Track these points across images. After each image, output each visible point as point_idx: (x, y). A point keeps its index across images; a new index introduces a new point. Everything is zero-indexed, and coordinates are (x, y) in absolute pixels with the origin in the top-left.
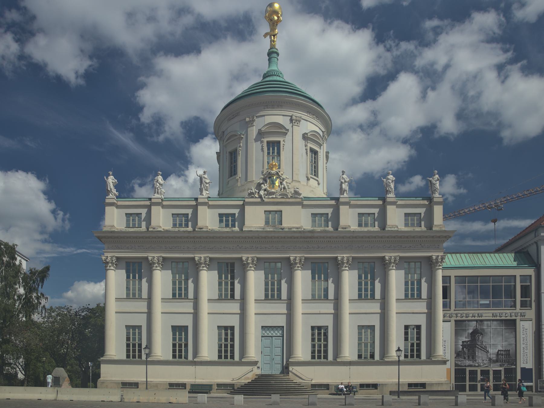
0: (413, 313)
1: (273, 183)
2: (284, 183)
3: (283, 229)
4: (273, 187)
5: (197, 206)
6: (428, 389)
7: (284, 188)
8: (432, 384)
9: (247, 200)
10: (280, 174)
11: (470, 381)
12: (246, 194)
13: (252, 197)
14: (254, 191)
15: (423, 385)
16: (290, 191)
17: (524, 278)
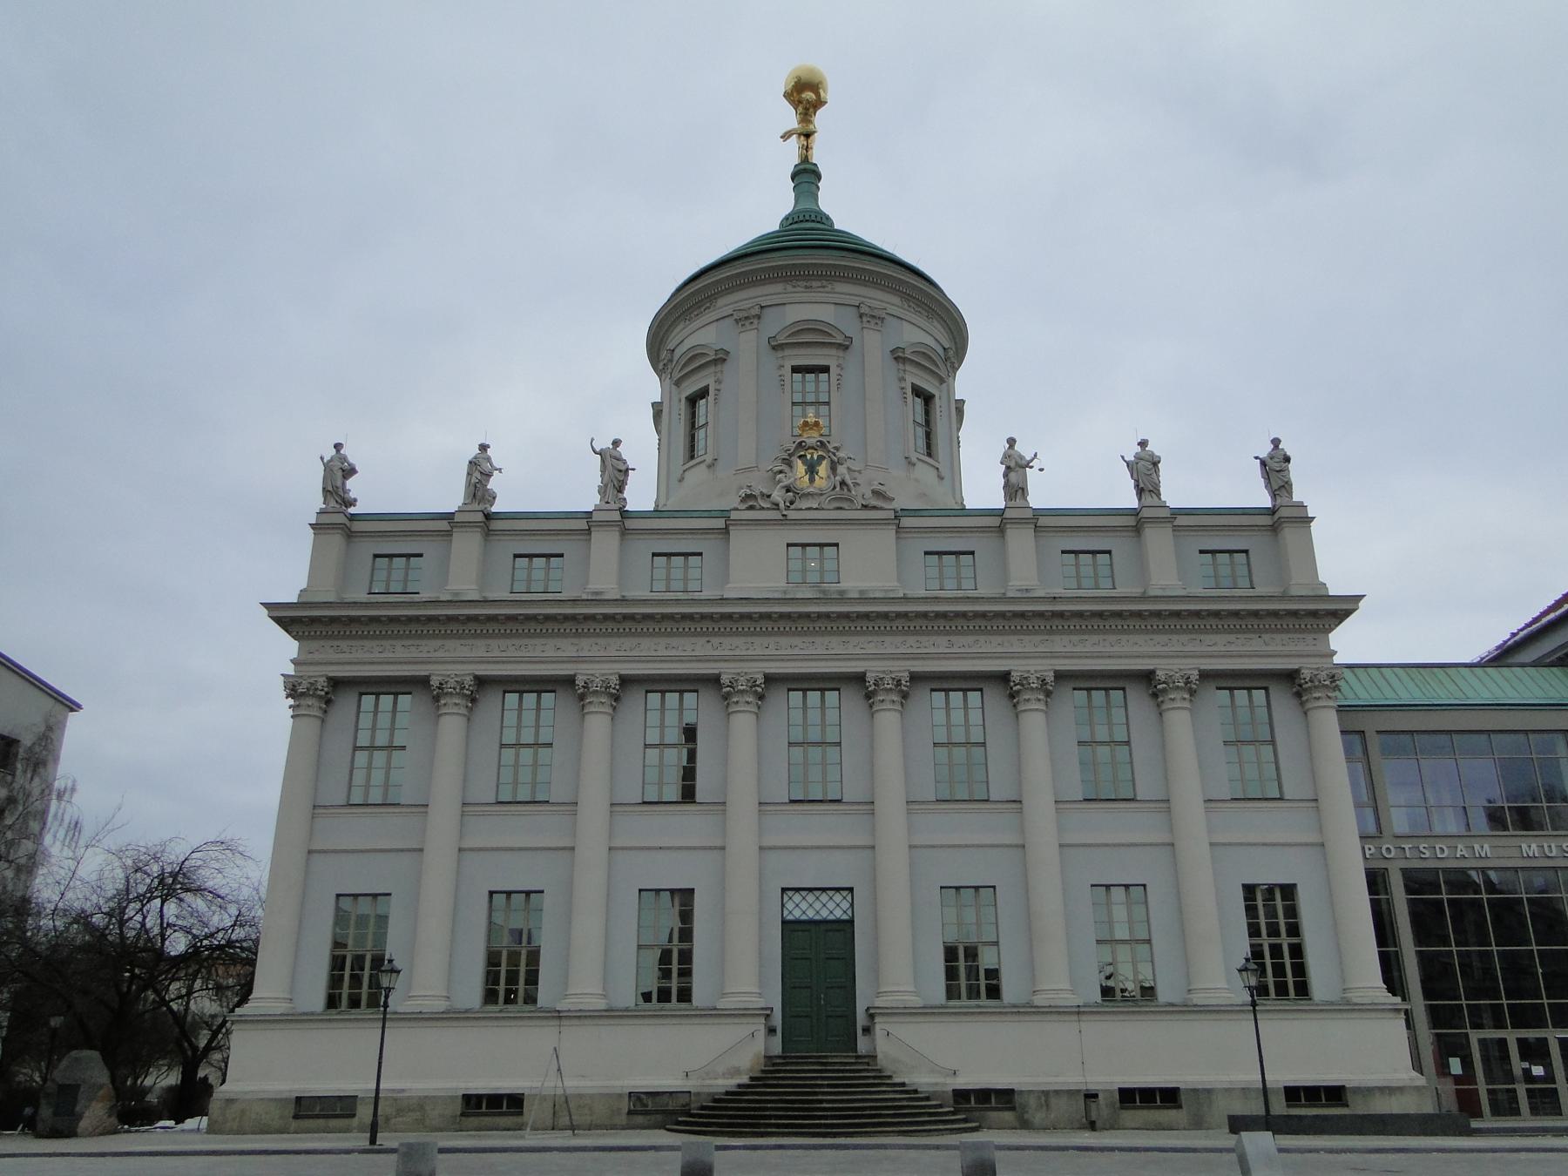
0: (1264, 844)
1: (812, 470)
2: (841, 469)
3: (842, 592)
4: (812, 480)
6: (1358, 1107)
7: (843, 483)
8: (1367, 1092)
9: (734, 515)
10: (830, 447)
12: (735, 502)
13: (751, 508)
14: (756, 493)
15: (1335, 1094)
16: (862, 493)
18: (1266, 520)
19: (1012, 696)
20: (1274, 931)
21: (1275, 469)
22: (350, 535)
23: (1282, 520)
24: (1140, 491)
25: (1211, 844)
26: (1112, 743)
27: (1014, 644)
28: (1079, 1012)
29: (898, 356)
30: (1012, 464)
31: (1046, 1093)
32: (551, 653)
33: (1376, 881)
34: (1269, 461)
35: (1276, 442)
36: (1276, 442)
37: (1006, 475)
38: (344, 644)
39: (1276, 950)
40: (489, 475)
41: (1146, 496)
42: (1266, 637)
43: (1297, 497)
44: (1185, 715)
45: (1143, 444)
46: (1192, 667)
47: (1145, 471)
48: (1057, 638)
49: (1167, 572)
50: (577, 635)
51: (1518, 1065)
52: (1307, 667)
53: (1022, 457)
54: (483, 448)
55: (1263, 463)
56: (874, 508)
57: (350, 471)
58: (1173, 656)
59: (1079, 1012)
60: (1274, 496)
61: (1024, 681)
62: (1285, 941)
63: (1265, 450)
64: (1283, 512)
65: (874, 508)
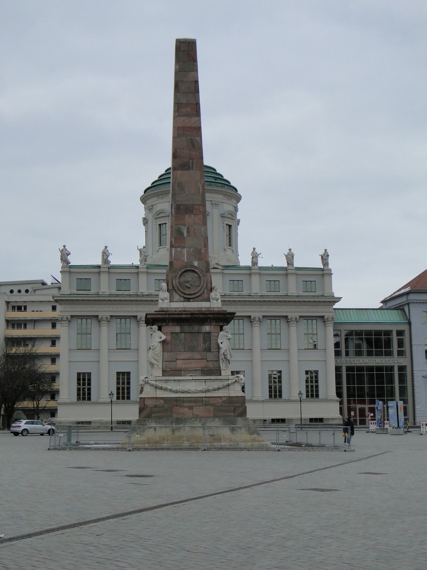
5: (138, 273)
8: (328, 419)
11: (360, 417)
15: (321, 420)
17: (400, 333)
18: (321, 273)
19: (251, 322)
20: (312, 382)
21: (325, 258)
22: (70, 272)
23: (324, 273)
24: (288, 264)
25: (299, 361)
26: (276, 334)
27: (252, 308)
28: (263, 402)
29: (223, 216)
30: (254, 256)
31: (255, 420)
32: (130, 310)
33: (338, 369)
34: (323, 256)
35: (326, 250)
36: (326, 250)
37: (252, 259)
38: (74, 306)
39: (312, 387)
40: (108, 256)
41: (289, 265)
42: (317, 307)
43: (330, 267)
44: (295, 327)
45: (290, 250)
46: (297, 315)
47: (290, 257)
48: (263, 307)
49: (293, 288)
50: (137, 304)
51: (367, 413)
52: (326, 315)
53: (257, 253)
54: (106, 247)
55: (322, 256)
56: (216, 268)
57: (69, 254)
58: (293, 312)
59: (263, 402)
60: (324, 266)
61: (254, 318)
62: (314, 384)
63: (322, 252)
64: (325, 272)
65: (216, 268)
